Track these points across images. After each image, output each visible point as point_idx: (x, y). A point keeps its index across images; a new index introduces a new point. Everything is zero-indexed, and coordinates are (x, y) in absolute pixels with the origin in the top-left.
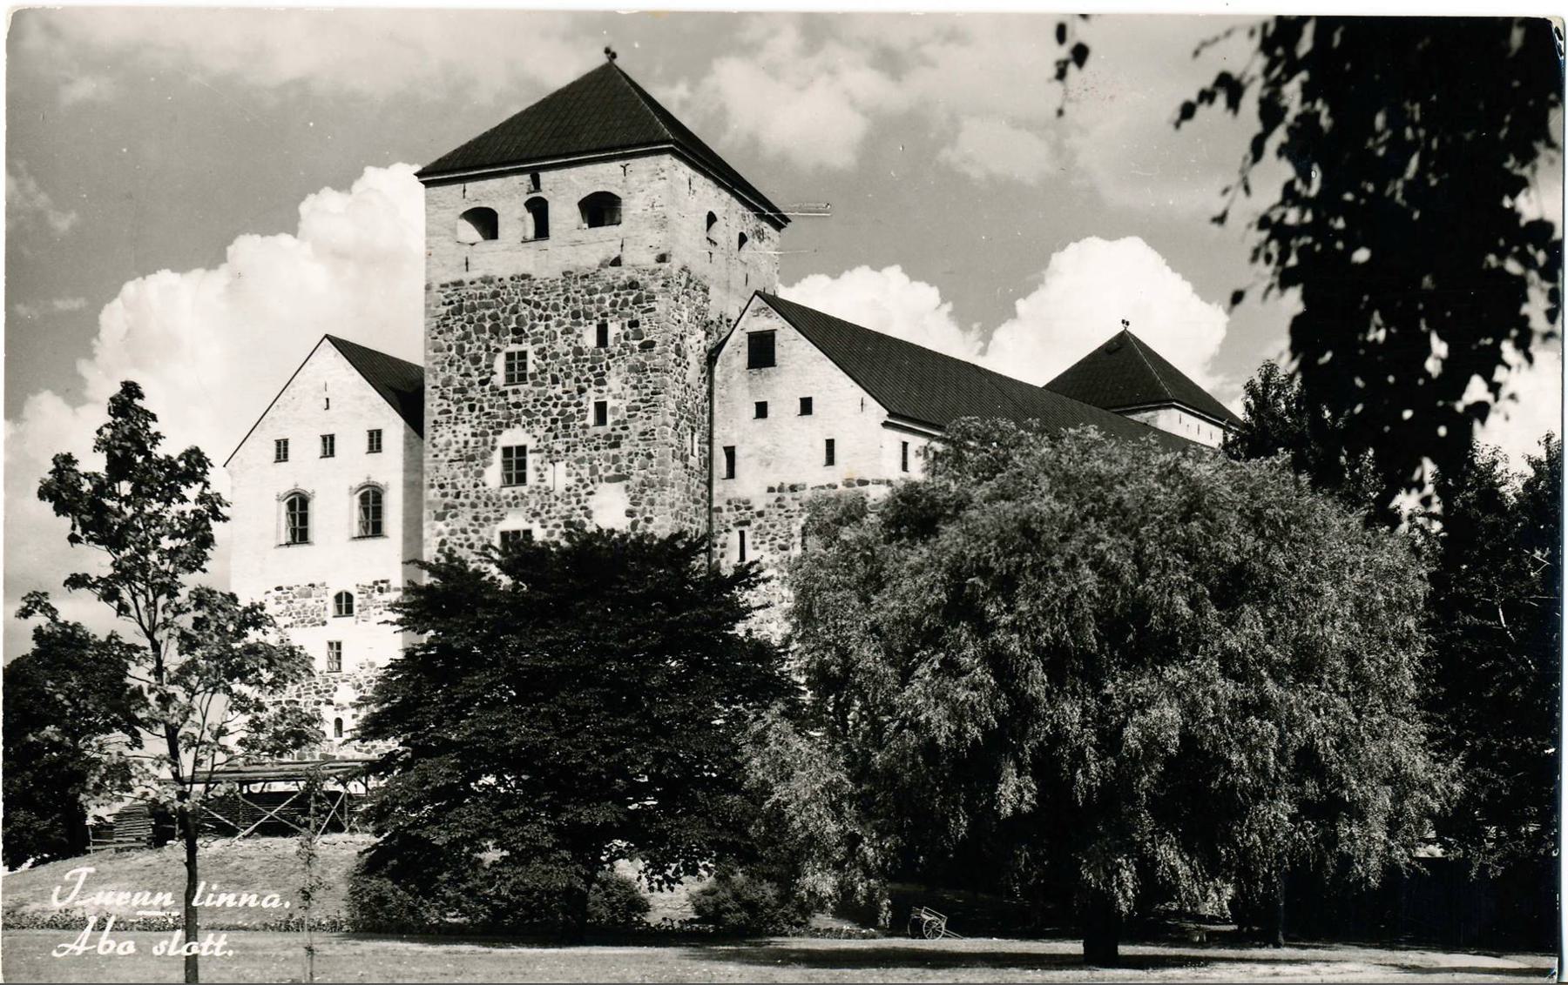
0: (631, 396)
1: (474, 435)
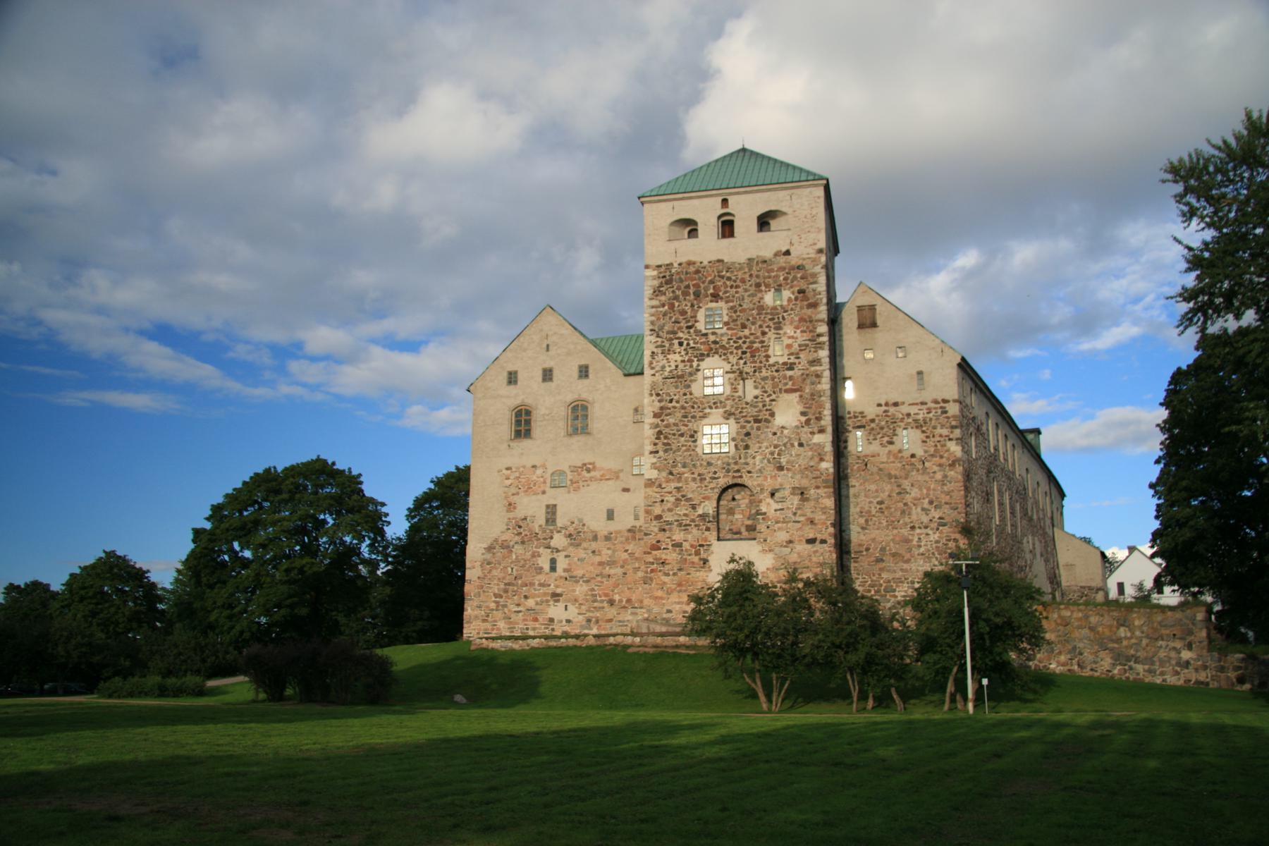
0: (801, 338)
1: (683, 361)
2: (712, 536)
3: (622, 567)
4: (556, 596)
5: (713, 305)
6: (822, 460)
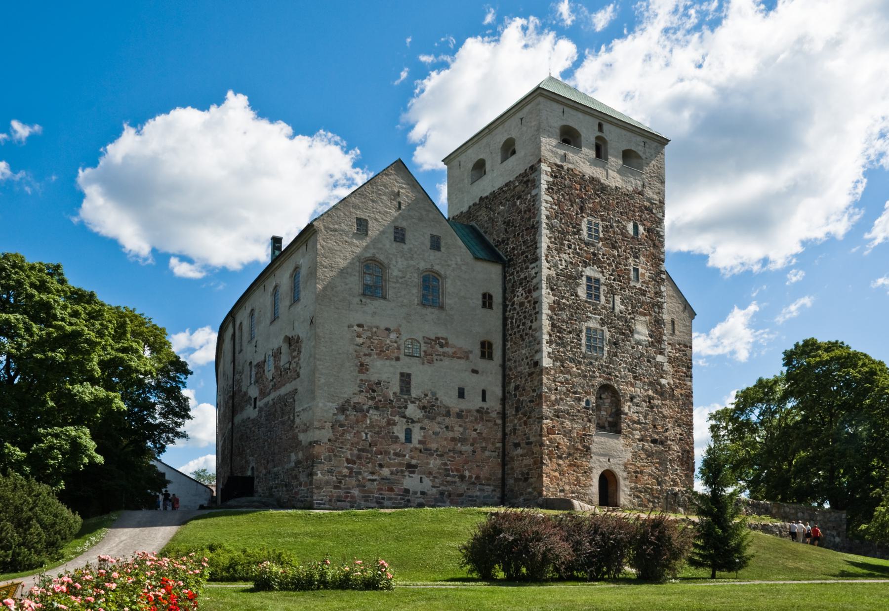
2: (593, 427)
3: (472, 445)
4: (411, 468)
5: (590, 218)
6: (662, 377)
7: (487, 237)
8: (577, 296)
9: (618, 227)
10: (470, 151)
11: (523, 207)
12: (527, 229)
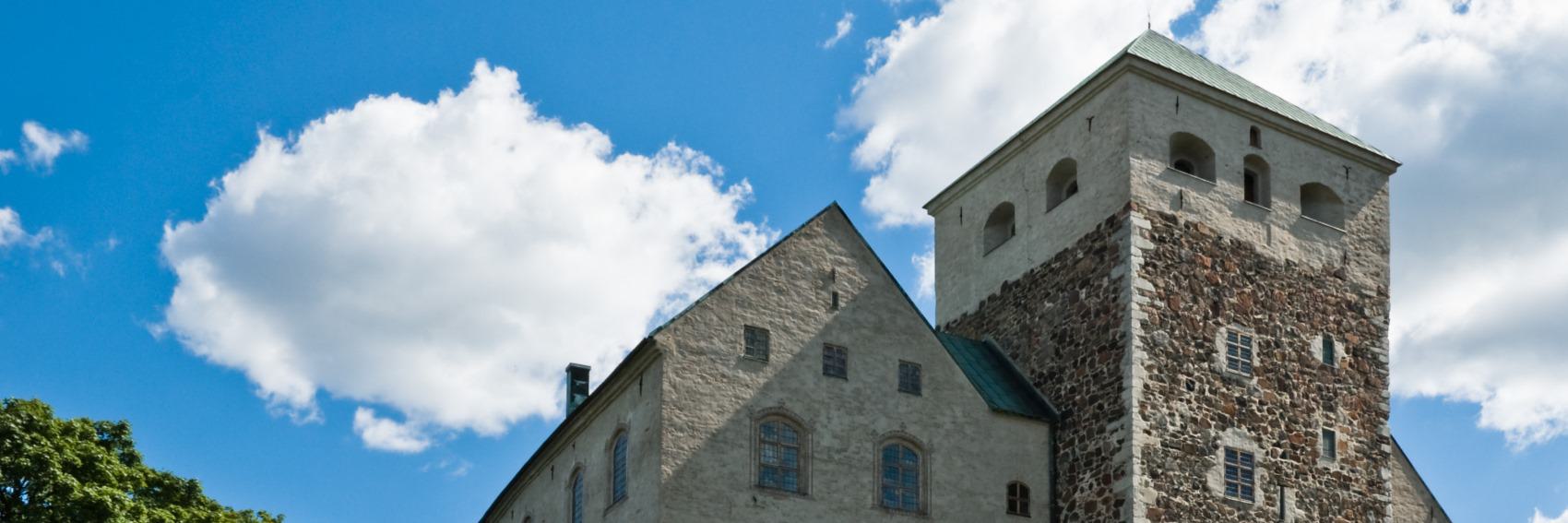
5: (1233, 327)
7: (1018, 367)
8: (1206, 489)
9: (1291, 344)
10: (981, 187)
11: (1093, 303)
12: (1102, 349)
